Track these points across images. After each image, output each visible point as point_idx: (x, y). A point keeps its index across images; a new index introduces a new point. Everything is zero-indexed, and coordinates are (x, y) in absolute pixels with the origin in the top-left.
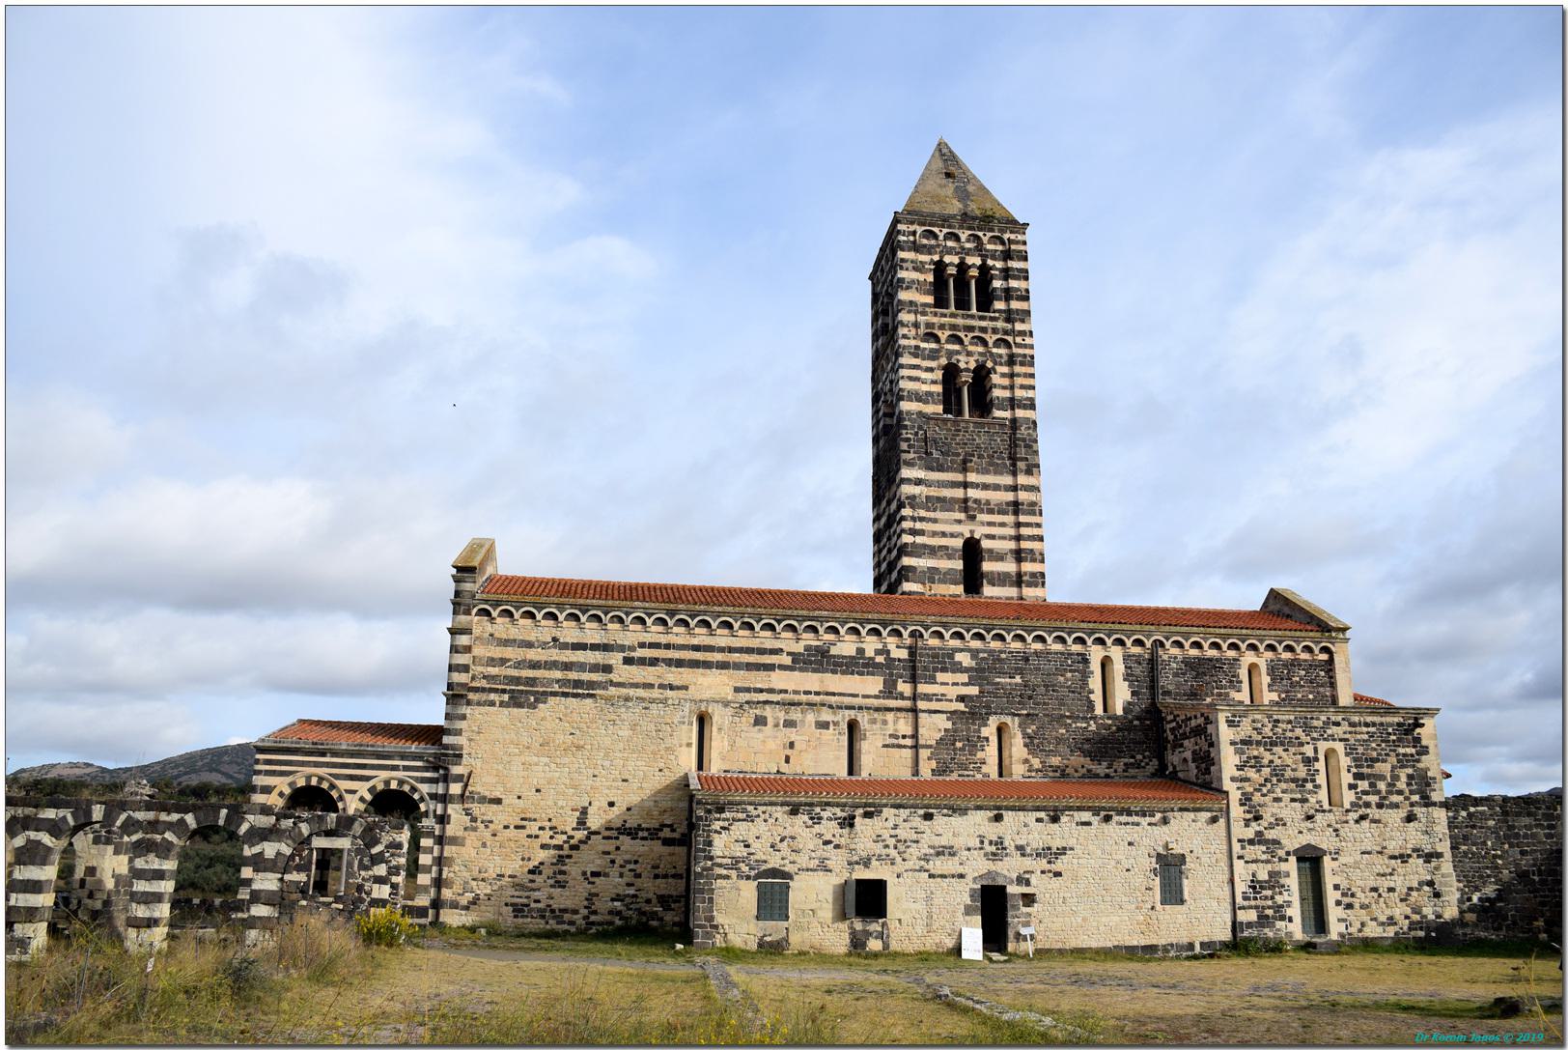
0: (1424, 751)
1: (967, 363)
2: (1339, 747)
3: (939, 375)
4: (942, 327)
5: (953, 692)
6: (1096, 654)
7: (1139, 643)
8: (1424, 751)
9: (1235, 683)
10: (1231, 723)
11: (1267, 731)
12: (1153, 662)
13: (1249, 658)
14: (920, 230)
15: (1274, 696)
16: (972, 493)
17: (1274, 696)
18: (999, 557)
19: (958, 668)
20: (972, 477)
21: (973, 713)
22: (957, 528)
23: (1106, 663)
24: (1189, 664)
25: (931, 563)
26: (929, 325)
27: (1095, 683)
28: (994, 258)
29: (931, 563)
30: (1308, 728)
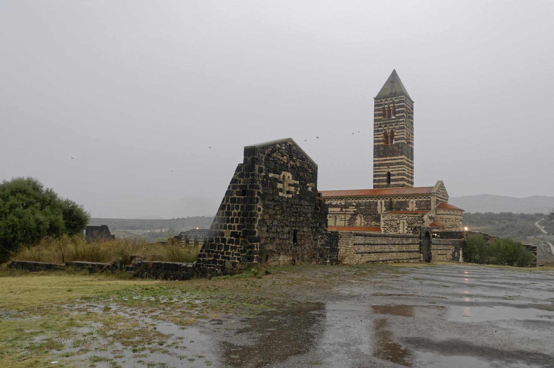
0: (424, 222)
1: (389, 131)
2: (405, 221)
3: (382, 135)
4: (383, 124)
5: (352, 210)
6: (379, 201)
7: (387, 199)
8: (424, 222)
9: (408, 206)
10: (383, 217)
11: (390, 218)
12: (391, 203)
13: (412, 200)
14: (379, 101)
15: (417, 208)
16: (388, 162)
17: (417, 208)
18: (394, 175)
19: (353, 206)
20: (388, 158)
21: (355, 215)
22: (385, 170)
23: (381, 203)
24: (397, 202)
25: (380, 178)
26: (380, 124)
27: (379, 207)
28: (396, 103)
29: (380, 178)
30: (398, 217)
